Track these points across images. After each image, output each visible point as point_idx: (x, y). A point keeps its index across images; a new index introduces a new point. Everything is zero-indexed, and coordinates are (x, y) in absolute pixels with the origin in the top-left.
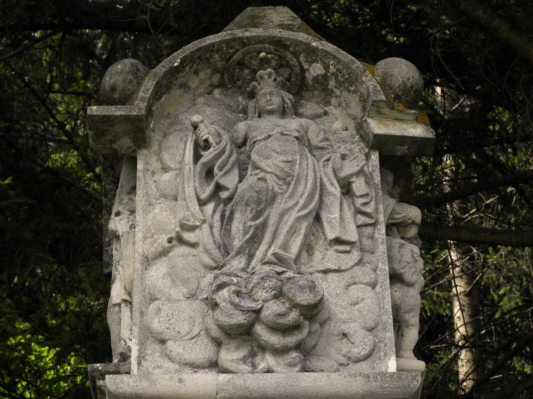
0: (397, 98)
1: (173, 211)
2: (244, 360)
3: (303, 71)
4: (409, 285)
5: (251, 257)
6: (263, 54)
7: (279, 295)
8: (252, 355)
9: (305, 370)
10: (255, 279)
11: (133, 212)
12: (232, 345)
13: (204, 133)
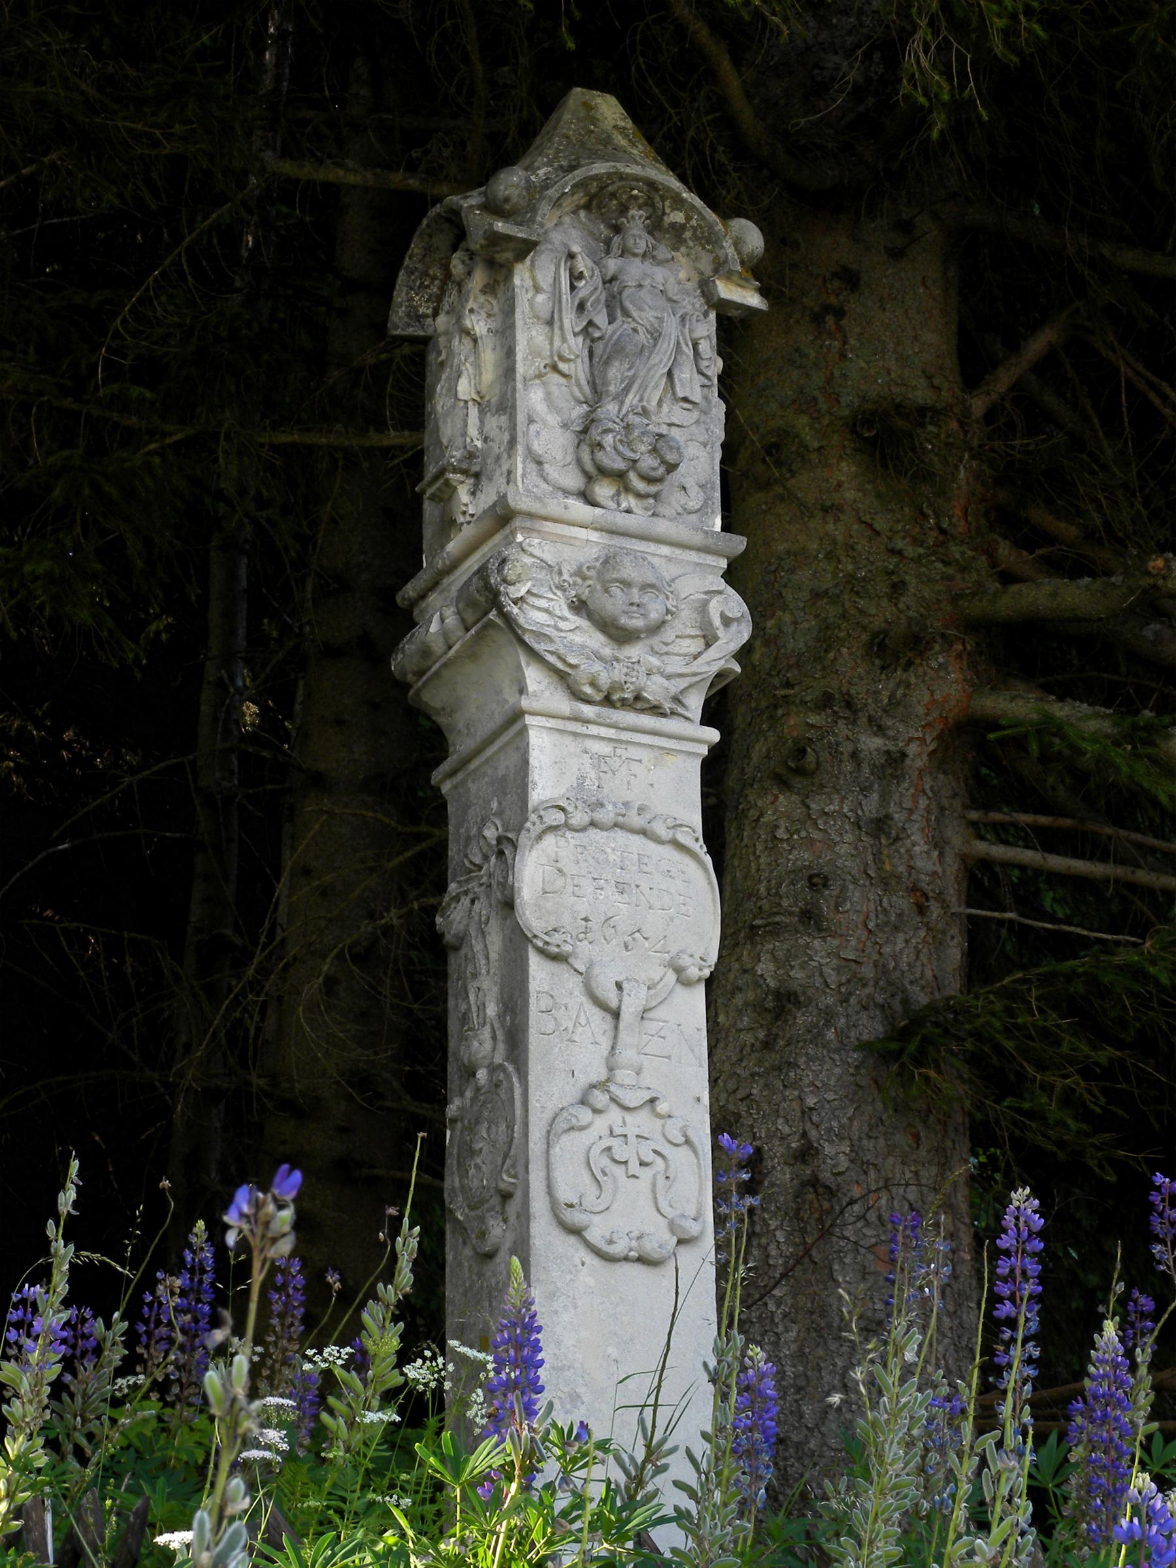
6: (635, 192)
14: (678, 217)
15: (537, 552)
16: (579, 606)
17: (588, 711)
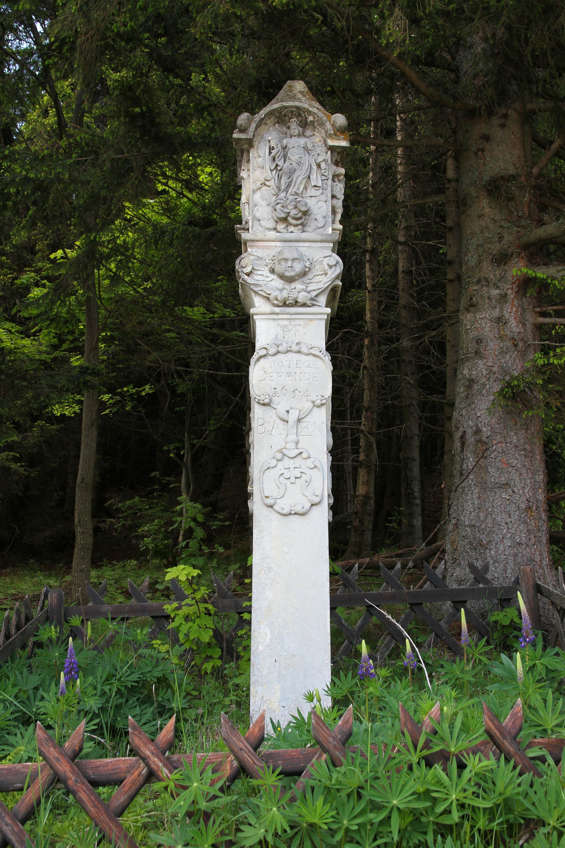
0: (338, 130)
1: (262, 173)
2: (284, 228)
3: (306, 118)
4: (338, 199)
5: (287, 192)
7: (296, 207)
8: (287, 226)
9: (303, 231)
10: (288, 202)
11: (248, 170)
12: (281, 223)
13: (273, 144)
14: (311, 118)
15: (255, 254)
16: (272, 271)
17: (277, 310)
